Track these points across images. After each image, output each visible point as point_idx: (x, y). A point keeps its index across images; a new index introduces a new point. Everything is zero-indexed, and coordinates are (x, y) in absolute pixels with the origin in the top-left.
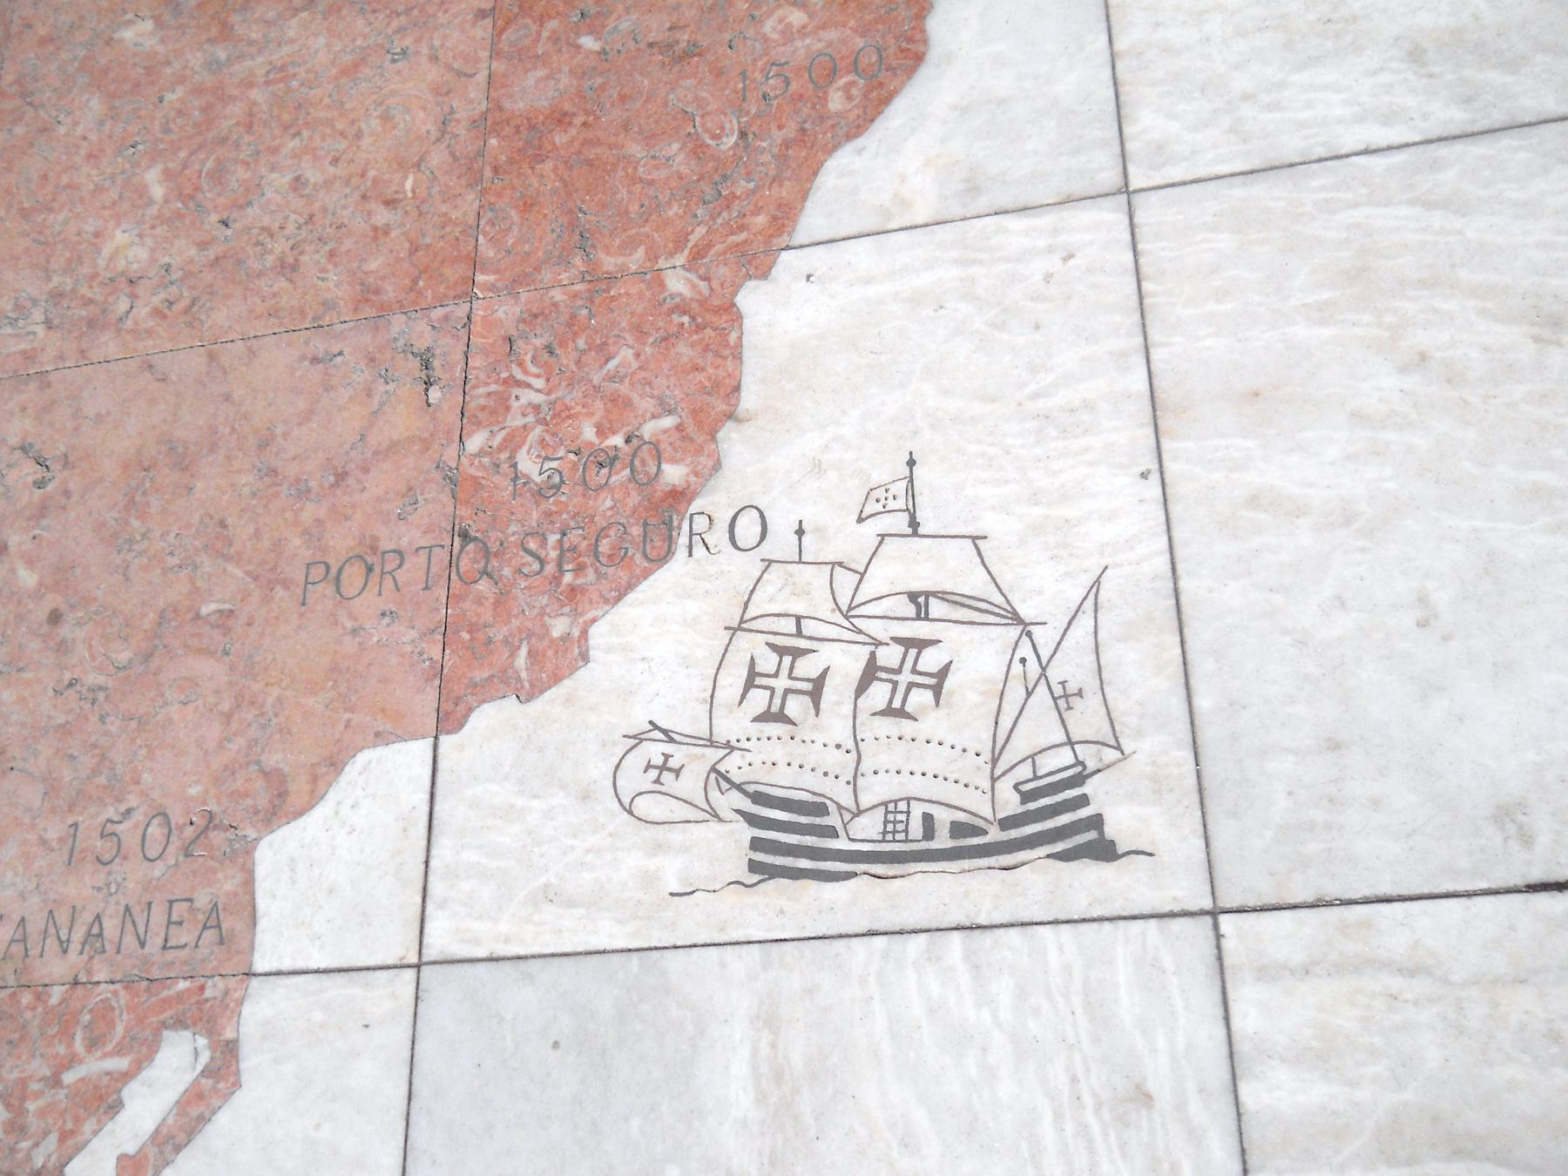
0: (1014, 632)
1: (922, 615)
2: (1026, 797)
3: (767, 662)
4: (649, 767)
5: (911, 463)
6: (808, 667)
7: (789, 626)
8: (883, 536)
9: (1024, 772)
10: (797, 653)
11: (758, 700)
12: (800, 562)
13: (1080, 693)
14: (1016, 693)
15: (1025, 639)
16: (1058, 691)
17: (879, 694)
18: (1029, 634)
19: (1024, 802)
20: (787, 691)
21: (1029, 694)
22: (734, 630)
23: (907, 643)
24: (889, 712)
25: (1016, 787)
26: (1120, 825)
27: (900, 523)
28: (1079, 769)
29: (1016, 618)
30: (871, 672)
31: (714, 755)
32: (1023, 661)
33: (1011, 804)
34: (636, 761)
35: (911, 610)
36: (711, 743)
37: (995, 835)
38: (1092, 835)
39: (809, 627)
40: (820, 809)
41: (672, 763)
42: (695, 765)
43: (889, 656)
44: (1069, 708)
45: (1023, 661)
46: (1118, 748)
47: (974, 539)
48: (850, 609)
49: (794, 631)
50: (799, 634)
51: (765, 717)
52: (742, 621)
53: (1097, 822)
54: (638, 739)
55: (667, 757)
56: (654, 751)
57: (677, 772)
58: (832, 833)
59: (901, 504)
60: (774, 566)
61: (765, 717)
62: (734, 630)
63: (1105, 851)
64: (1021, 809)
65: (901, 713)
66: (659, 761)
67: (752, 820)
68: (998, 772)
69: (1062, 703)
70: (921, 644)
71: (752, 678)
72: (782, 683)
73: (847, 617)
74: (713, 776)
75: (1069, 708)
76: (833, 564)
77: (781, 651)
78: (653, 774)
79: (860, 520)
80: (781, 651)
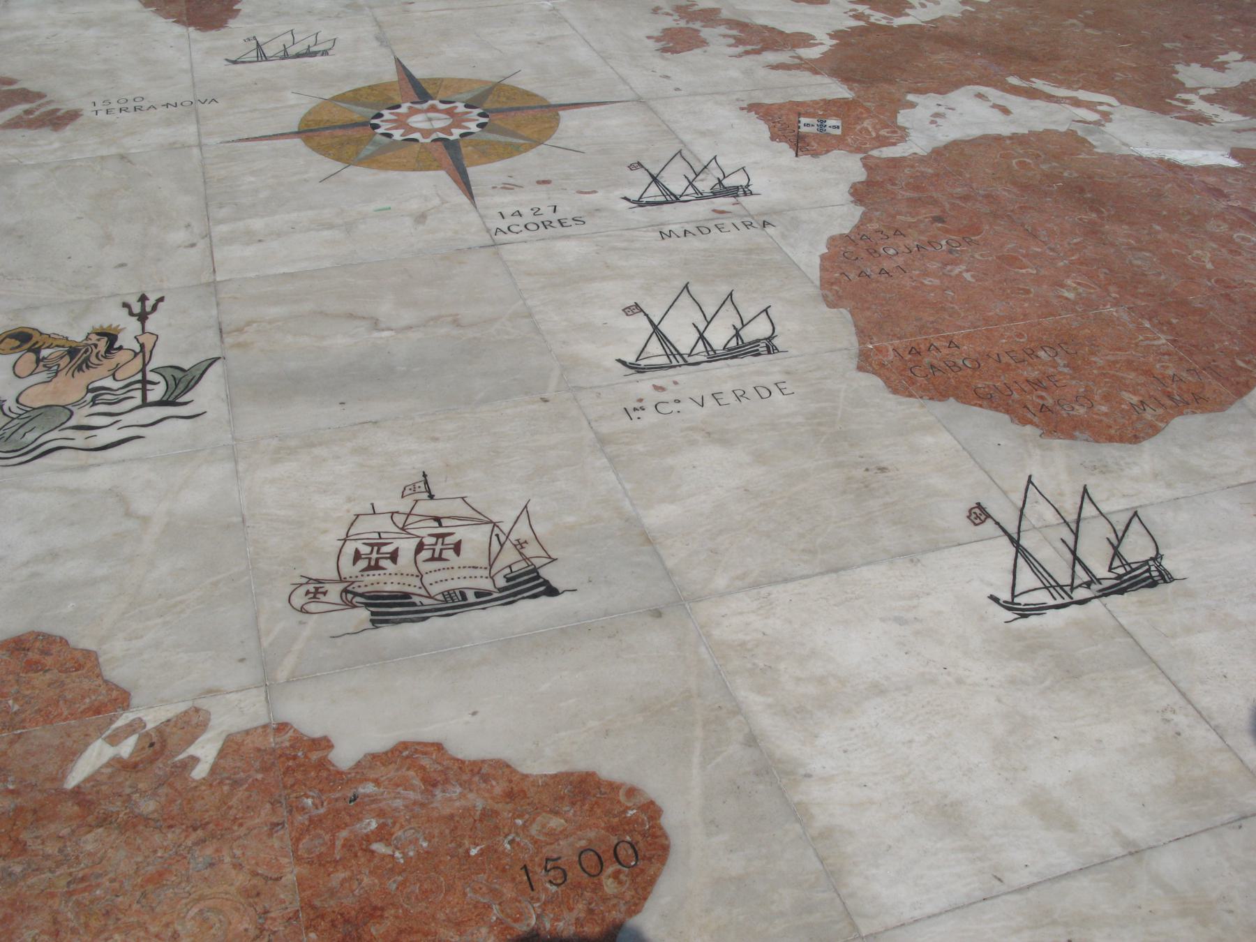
0: (490, 527)
1: (440, 525)
2: (508, 580)
3: (365, 550)
4: (308, 593)
5: (425, 475)
6: (388, 549)
7: (376, 536)
8: (417, 501)
9: (508, 571)
10: (380, 545)
11: (362, 564)
12: (375, 513)
13: (526, 542)
14: (496, 546)
15: (496, 528)
16: (516, 543)
17: (425, 554)
18: (498, 526)
19: (507, 581)
20: (377, 560)
21: (502, 545)
22: (345, 540)
23: (438, 536)
24: (432, 559)
25: (505, 577)
26: (556, 583)
27: (426, 495)
28: (532, 567)
29: (491, 522)
30: (420, 547)
31: (346, 584)
32: (497, 535)
33: (501, 582)
34: (303, 590)
35: (436, 524)
36: (341, 580)
37: (495, 595)
38: (542, 589)
39: (383, 535)
40: (407, 595)
41: (320, 590)
42: (334, 592)
43: (429, 541)
44: (522, 548)
45: (497, 535)
46: (550, 557)
47: (463, 498)
48: (404, 526)
49: (378, 537)
50: (380, 538)
51: (369, 568)
52: (347, 536)
53: (546, 582)
54: (301, 585)
55: (317, 589)
56: (311, 588)
57: (325, 593)
58: (414, 604)
59: (423, 489)
60: (360, 517)
61: (369, 568)
62: (345, 540)
63: (552, 592)
64: (507, 584)
65: (440, 559)
66: (313, 590)
67: (367, 605)
68: (493, 572)
69: (519, 547)
70: (443, 536)
71: (357, 556)
72: (374, 555)
73: (404, 530)
74: (344, 594)
75: (522, 548)
76: (393, 513)
77: (372, 545)
78: (312, 595)
79: (403, 497)
80: (372, 545)
